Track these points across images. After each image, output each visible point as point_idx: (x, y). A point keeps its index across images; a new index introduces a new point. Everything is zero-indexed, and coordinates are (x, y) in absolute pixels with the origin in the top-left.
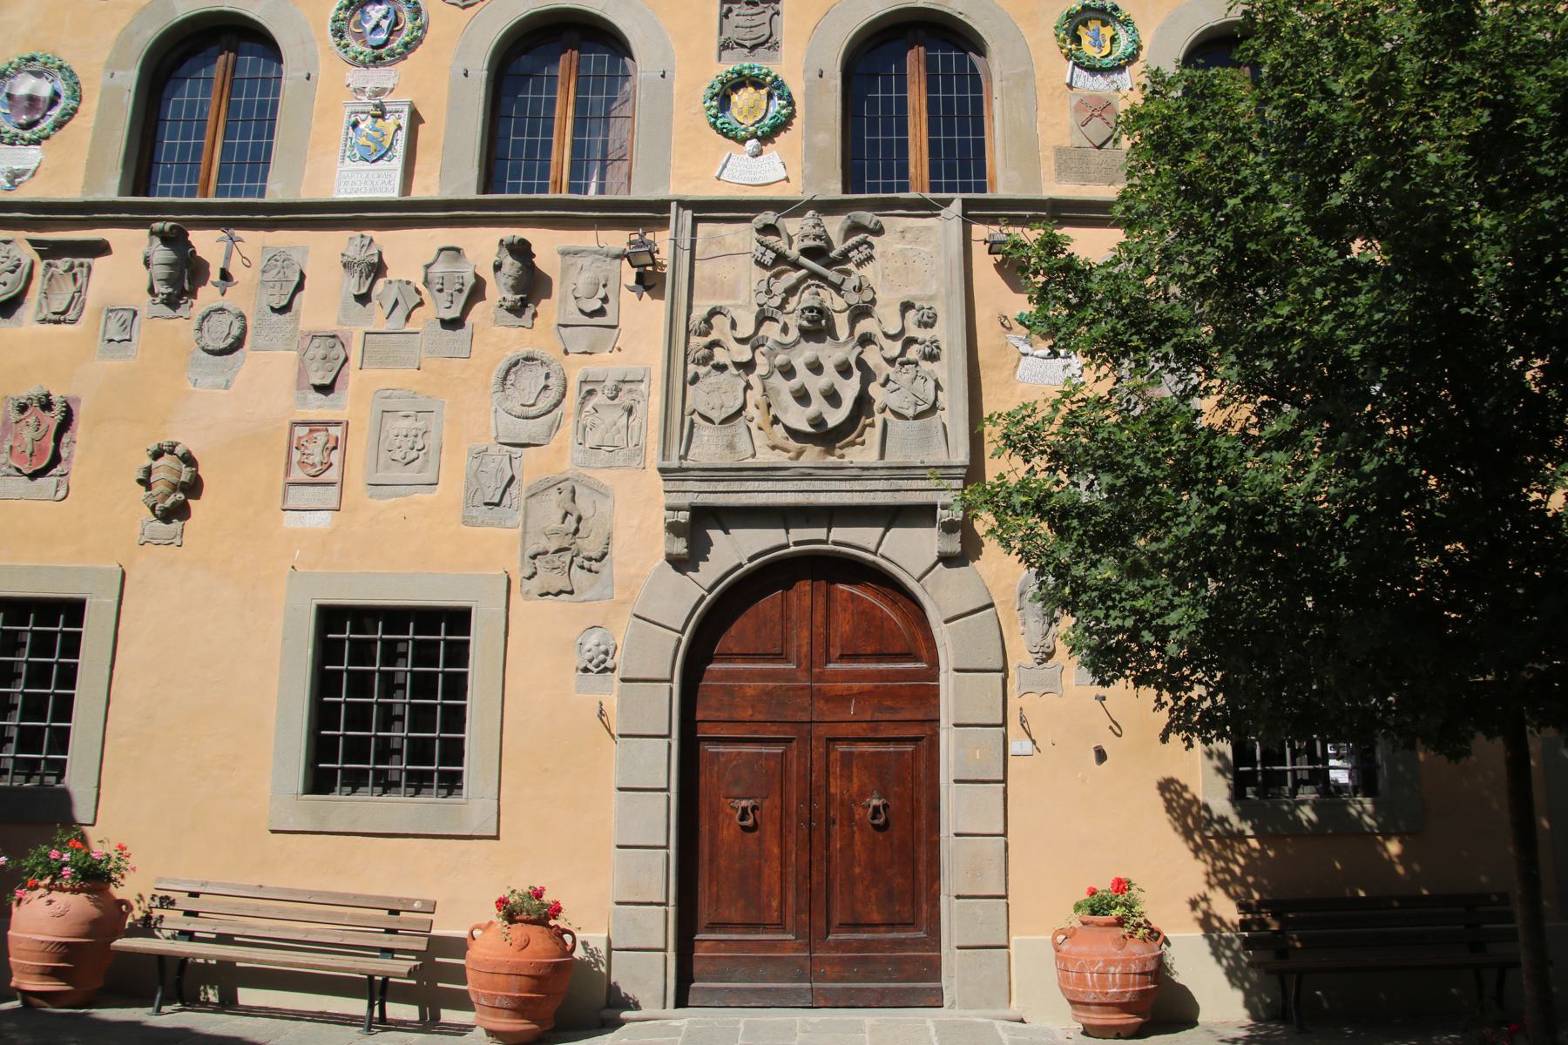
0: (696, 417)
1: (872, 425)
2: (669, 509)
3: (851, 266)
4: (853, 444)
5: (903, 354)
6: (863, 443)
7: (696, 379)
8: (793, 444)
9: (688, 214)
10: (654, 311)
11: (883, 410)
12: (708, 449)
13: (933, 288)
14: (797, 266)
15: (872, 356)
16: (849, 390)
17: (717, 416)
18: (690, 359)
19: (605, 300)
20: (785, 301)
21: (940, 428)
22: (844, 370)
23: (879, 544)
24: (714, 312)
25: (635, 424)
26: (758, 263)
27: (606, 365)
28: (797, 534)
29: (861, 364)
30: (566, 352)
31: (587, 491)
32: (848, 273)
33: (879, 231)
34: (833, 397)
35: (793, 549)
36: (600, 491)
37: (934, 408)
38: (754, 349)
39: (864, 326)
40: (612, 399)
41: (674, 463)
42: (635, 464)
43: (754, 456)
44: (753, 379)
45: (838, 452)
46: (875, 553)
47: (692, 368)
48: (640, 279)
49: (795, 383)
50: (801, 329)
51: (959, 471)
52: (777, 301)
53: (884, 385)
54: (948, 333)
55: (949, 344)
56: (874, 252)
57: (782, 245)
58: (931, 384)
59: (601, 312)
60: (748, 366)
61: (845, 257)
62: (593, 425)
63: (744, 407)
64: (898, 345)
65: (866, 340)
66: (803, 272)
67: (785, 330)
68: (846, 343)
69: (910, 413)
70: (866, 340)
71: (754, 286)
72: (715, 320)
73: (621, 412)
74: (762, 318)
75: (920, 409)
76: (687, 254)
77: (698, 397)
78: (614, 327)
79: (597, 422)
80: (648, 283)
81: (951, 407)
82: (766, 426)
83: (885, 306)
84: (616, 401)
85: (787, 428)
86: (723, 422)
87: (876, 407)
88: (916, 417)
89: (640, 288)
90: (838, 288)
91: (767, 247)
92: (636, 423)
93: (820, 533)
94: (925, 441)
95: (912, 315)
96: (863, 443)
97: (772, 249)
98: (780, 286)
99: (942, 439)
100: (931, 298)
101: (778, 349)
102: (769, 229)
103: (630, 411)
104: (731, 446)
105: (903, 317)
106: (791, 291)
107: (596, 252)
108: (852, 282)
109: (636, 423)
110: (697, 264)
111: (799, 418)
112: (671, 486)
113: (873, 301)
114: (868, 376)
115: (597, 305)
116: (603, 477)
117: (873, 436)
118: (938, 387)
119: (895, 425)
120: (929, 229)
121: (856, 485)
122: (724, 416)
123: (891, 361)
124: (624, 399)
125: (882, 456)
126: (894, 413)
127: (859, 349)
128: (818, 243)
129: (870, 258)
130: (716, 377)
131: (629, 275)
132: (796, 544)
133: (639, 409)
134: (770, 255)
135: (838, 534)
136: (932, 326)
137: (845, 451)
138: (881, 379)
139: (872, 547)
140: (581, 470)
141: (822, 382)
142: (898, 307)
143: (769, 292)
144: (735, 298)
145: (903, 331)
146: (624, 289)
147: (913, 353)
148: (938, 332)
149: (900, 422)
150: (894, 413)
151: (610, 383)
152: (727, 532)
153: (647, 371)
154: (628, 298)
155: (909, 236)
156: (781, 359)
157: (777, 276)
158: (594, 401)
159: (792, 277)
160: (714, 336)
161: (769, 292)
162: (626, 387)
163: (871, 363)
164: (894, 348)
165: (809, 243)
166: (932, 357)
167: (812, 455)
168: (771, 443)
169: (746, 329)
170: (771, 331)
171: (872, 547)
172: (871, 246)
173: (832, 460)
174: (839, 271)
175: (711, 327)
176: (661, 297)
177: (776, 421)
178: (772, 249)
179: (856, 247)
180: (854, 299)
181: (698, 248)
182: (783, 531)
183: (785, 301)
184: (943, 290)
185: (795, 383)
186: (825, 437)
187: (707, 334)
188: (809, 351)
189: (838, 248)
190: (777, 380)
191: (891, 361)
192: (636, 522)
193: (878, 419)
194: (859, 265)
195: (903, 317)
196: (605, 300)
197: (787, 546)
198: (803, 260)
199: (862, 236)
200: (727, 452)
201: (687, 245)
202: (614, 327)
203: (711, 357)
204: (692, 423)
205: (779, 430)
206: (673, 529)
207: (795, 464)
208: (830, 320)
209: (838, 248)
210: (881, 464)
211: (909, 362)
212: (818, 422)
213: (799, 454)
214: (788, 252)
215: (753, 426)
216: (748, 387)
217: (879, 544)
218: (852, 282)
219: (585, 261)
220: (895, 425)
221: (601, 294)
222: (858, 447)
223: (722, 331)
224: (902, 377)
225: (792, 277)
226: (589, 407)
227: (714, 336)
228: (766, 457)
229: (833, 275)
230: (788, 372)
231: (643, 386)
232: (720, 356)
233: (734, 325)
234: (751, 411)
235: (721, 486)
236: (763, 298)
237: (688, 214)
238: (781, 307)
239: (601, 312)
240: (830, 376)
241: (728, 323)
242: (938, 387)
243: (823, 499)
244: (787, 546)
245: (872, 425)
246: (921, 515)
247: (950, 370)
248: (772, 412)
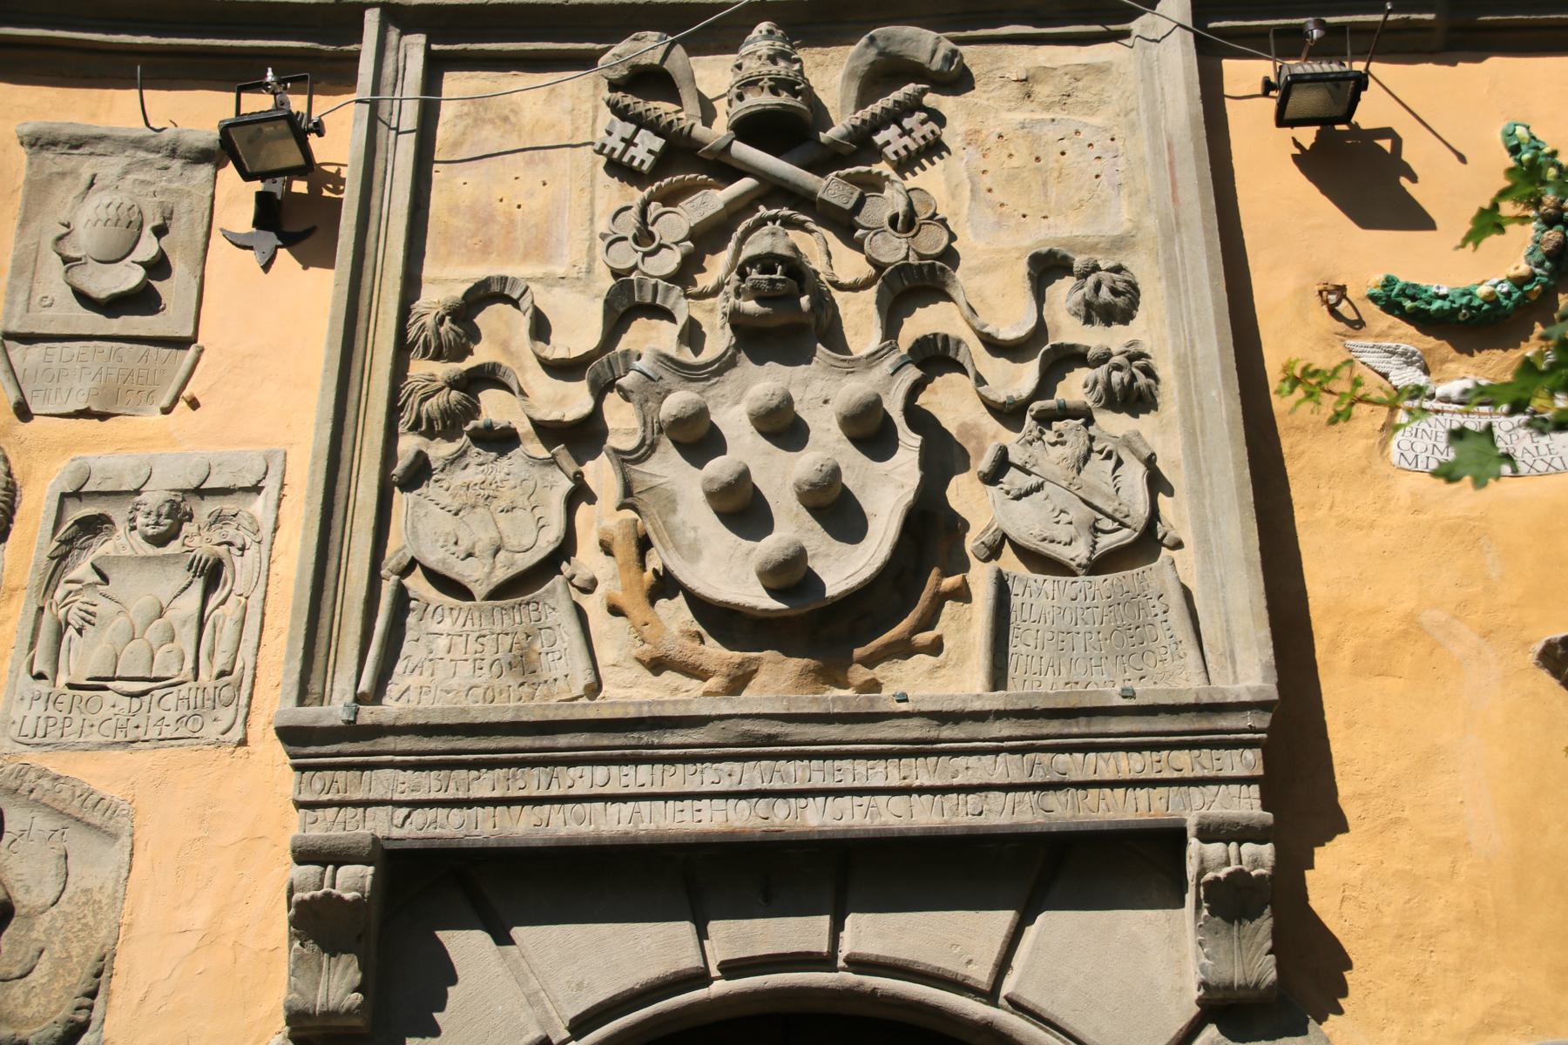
0: (416, 583)
1: (962, 594)
2: (304, 856)
3: (883, 168)
4: (904, 649)
5: (1045, 387)
6: (936, 648)
7: (420, 471)
8: (714, 652)
9: (414, 48)
10: (308, 294)
11: (993, 552)
12: (447, 668)
13: (1119, 217)
14: (724, 169)
15: (951, 402)
16: (888, 490)
17: (479, 575)
18: (407, 417)
19: (159, 267)
20: (689, 267)
21: (1175, 598)
22: (870, 432)
23: (1003, 965)
24: (484, 294)
25: (225, 615)
26: (618, 168)
27: (150, 449)
28: (734, 937)
29: (920, 420)
30: (23, 412)
31: (42, 823)
32: (874, 184)
33: (958, 81)
34: (837, 510)
35: (720, 987)
36: (89, 818)
37: (1147, 543)
38: (600, 391)
39: (924, 321)
40: (160, 540)
41: (335, 710)
42: (212, 731)
43: (594, 689)
44: (600, 473)
45: (859, 674)
46: (990, 996)
47: (408, 444)
48: (269, 213)
49: (719, 468)
50: (737, 320)
51: (1248, 720)
52: (669, 261)
53: (993, 477)
54: (1174, 330)
55: (1185, 366)
56: (947, 136)
57: (686, 116)
58: (1134, 474)
59: (142, 300)
60: (582, 437)
61: (862, 144)
62: (89, 618)
63: (566, 548)
64: (1026, 376)
65: (935, 357)
66: (746, 183)
67: (692, 335)
68: (874, 357)
69: (1079, 552)
70: (935, 357)
71: (603, 225)
72: (489, 319)
73: (180, 576)
74: (626, 306)
75: (1106, 542)
76: (407, 145)
77: (422, 526)
78: (182, 343)
79: (104, 607)
80: (291, 227)
81: (1203, 539)
82: (634, 602)
83: (985, 269)
84: (174, 547)
85: (702, 607)
86: (500, 592)
87: (971, 543)
88: (1101, 564)
89: (271, 239)
90: (844, 224)
91: (640, 122)
92: (232, 609)
93: (803, 932)
94: (1130, 635)
95: (1063, 292)
96: (936, 648)
97: (655, 127)
98: (676, 224)
99: (1183, 630)
100: (1120, 243)
101: (669, 378)
102: (654, 80)
103: (212, 574)
104: (523, 665)
105: (1040, 299)
106: (708, 237)
107: (138, 144)
108: (892, 201)
109: (232, 609)
110: (439, 174)
111: (731, 571)
112: (318, 786)
113: (950, 256)
114: (943, 457)
115: (128, 277)
116: (102, 774)
117: (966, 627)
118: (1157, 483)
119: (1036, 596)
120: (1100, 70)
121: (922, 772)
122: (501, 575)
123: (1009, 414)
124: (199, 540)
125: (998, 678)
126: (1028, 556)
127: (912, 374)
128: (784, 98)
129: (934, 148)
130: (480, 469)
131: (236, 198)
132: (732, 969)
133: (241, 571)
134: (647, 145)
135: (868, 933)
136: (1126, 316)
137: (879, 672)
138: (984, 463)
139: (981, 974)
140: (34, 757)
141: (804, 464)
142: (1023, 268)
143: (644, 236)
144: (546, 259)
145: (1040, 331)
146: (217, 241)
147: (1075, 387)
148: (1148, 331)
149: (1049, 582)
150: (1028, 556)
151: (154, 497)
152: (502, 938)
153: (275, 462)
154: (231, 267)
155: (1042, 91)
156: (678, 401)
157: (670, 198)
158: (103, 548)
159: (716, 199)
160: (481, 355)
161: (644, 236)
162: (204, 509)
163: (949, 422)
164: (1021, 378)
165: (760, 99)
166: (1134, 398)
167: (778, 682)
168: (647, 651)
169: (578, 332)
170: (650, 339)
171: (981, 974)
172: (938, 118)
173: (837, 697)
174: (851, 180)
175: (474, 335)
176: (328, 261)
177: (665, 585)
178: (655, 127)
179: (893, 117)
180: (893, 249)
181: (442, 133)
182: (686, 929)
183: (689, 267)
184: (1151, 223)
185: (719, 468)
186: (818, 627)
187: (461, 353)
188: (764, 382)
189: (842, 119)
190: (667, 467)
191: (1009, 414)
192: (200, 916)
193: (980, 578)
194: (906, 164)
195: (1040, 299)
196: (159, 267)
197: (700, 978)
198: (742, 150)
199: (910, 88)
200: (510, 680)
201: (409, 117)
202: (182, 343)
203: (473, 410)
204: (402, 600)
205: (675, 613)
206: (316, 923)
207: (725, 706)
208: (824, 304)
209: (842, 119)
210: (996, 701)
211: (1065, 412)
212: (793, 577)
213: (738, 682)
214: (700, 130)
215: (593, 605)
216: (580, 494)
217: (1003, 965)
218: (892, 201)
219: (109, 167)
220: (1036, 596)
221: (148, 248)
222: (922, 661)
223: (505, 346)
224: (1049, 456)
225: (716, 199)
226: (82, 569)
227: (481, 355)
228: (630, 691)
229: (832, 188)
230: (699, 440)
231: (259, 506)
232: (494, 407)
233: (540, 328)
234: (587, 561)
235: (485, 784)
236: (626, 256)
237: (414, 48)
238: (684, 275)
239: (142, 300)
240: (827, 444)
241: (523, 322)
242: (1157, 483)
243: (816, 817)
244: (700, 978)
245: (962, 594)
246: (1134, 865)
247: (1191, 431)
248: (654, 561)
